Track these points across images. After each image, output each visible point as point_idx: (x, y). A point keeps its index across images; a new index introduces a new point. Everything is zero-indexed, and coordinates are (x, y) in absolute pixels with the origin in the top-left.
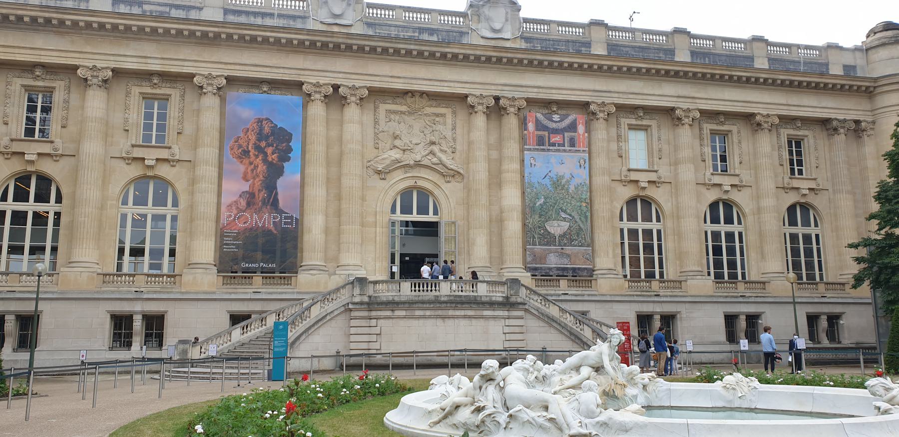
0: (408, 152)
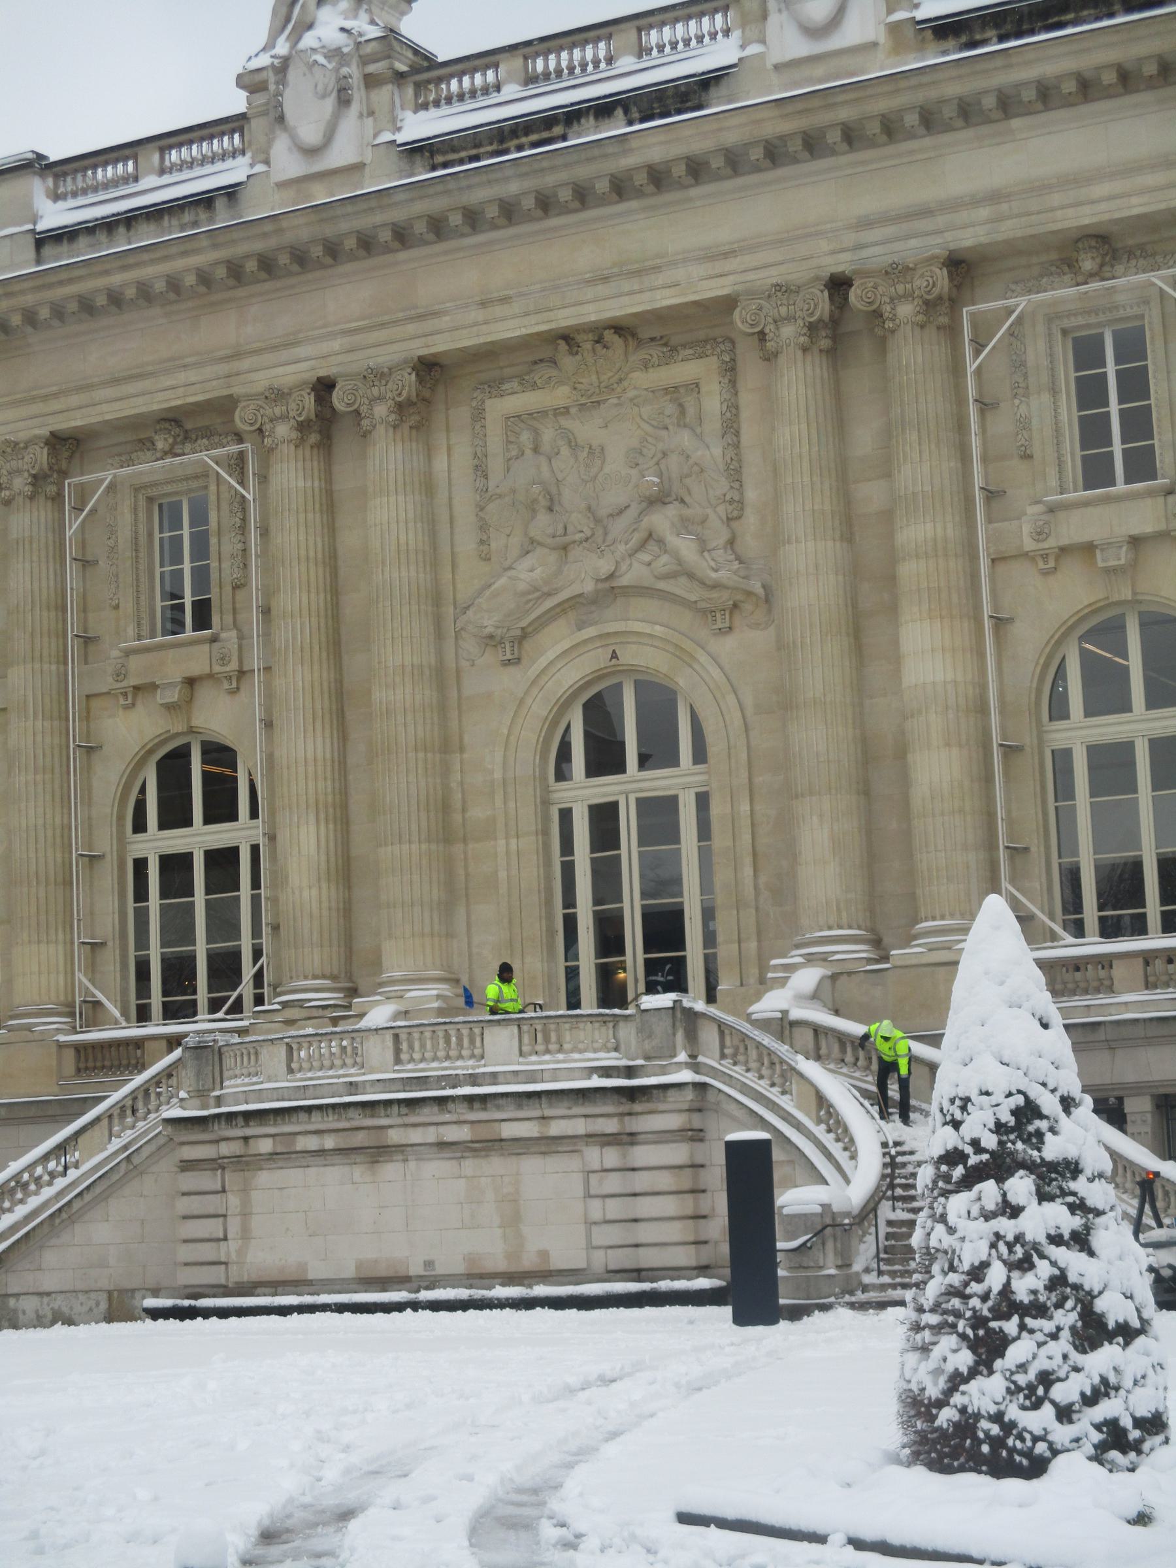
0: (575, 552)
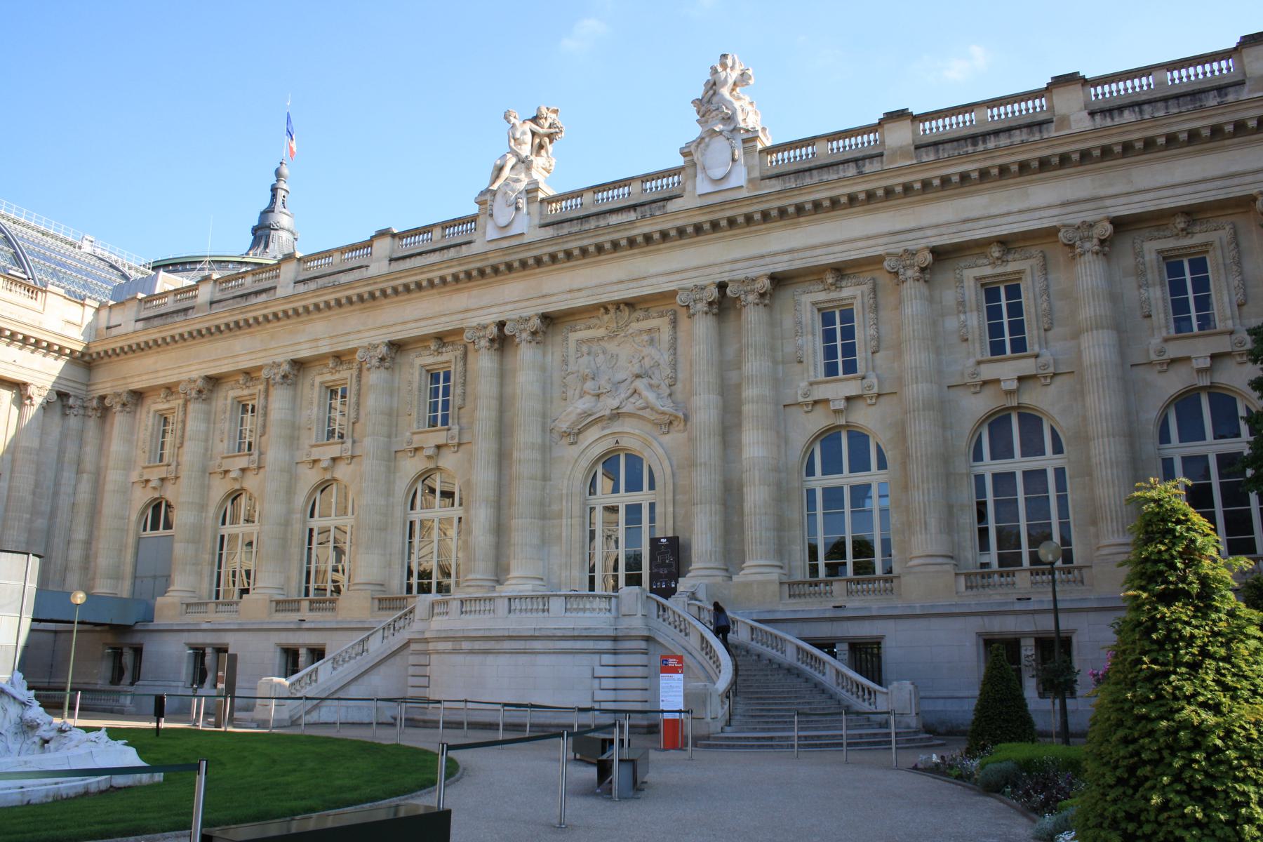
0: (602, 398)
